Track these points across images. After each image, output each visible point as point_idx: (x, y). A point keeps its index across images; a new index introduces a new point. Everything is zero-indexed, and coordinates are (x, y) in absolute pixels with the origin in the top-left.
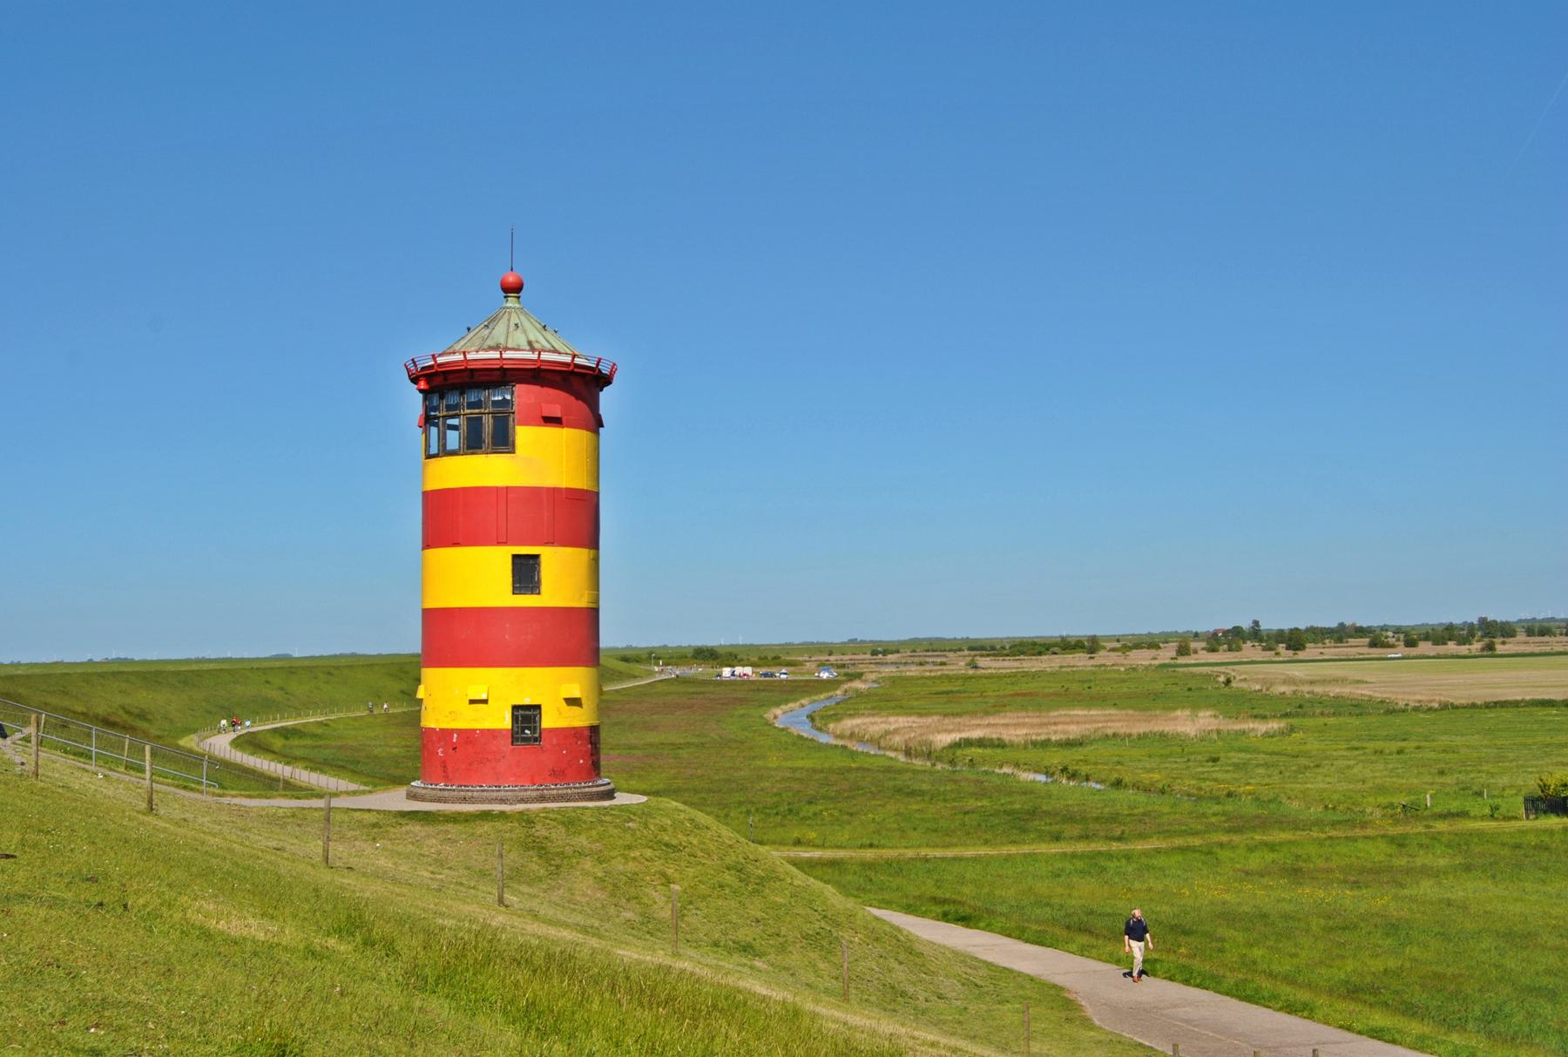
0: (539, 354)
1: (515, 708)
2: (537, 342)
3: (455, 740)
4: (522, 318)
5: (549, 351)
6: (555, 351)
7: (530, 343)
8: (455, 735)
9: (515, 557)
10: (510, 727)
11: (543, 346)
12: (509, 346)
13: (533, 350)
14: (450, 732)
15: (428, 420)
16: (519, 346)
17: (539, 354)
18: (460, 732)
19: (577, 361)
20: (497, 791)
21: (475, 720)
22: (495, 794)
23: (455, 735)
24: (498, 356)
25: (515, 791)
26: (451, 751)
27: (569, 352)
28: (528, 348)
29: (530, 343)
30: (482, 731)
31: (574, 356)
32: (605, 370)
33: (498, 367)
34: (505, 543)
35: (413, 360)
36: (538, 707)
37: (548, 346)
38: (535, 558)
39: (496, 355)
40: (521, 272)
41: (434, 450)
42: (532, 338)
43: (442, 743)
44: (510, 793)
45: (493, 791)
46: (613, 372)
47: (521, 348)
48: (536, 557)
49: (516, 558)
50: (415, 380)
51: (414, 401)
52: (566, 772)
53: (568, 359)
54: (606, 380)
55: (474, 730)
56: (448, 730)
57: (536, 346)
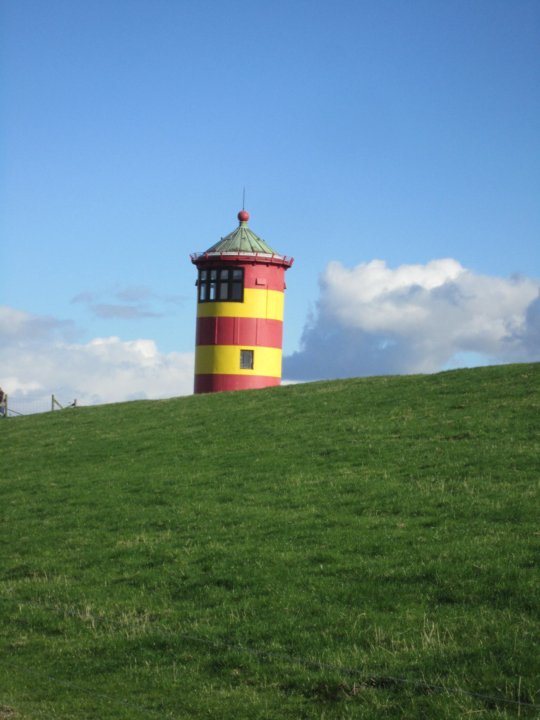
0: (257, 254)
2: (256, 247)
4: (248, 234)
5: (261, 252)
6: (265, 252)
7: (252, 248)
9: (242, 351)
11: (258, 249)
12: (242, 249)
13: (253, 251)
15: (199, 283)
16: (247, 249)
17: (257, 254)
19: (275, 257)
24: (237, 255)
27: (271, 252)
28: (251, 250)
29: (252, 248)
31: (273, 254)
32: (288, 260)
33: (235, 260)
34: (236, 344)
35: (195, 253)
37: (261, 249)
38: (252, 352)
39: (236, 254)
40: (249, 212)
41: (202, 298)
42: (253, 245)
46: (292, 260)
47: (248, 250)
48: (252, 352)
50: (194, 262)
51: (193, 272)
53: (270, 256)
54: (289, 267)
57: (255, 249)
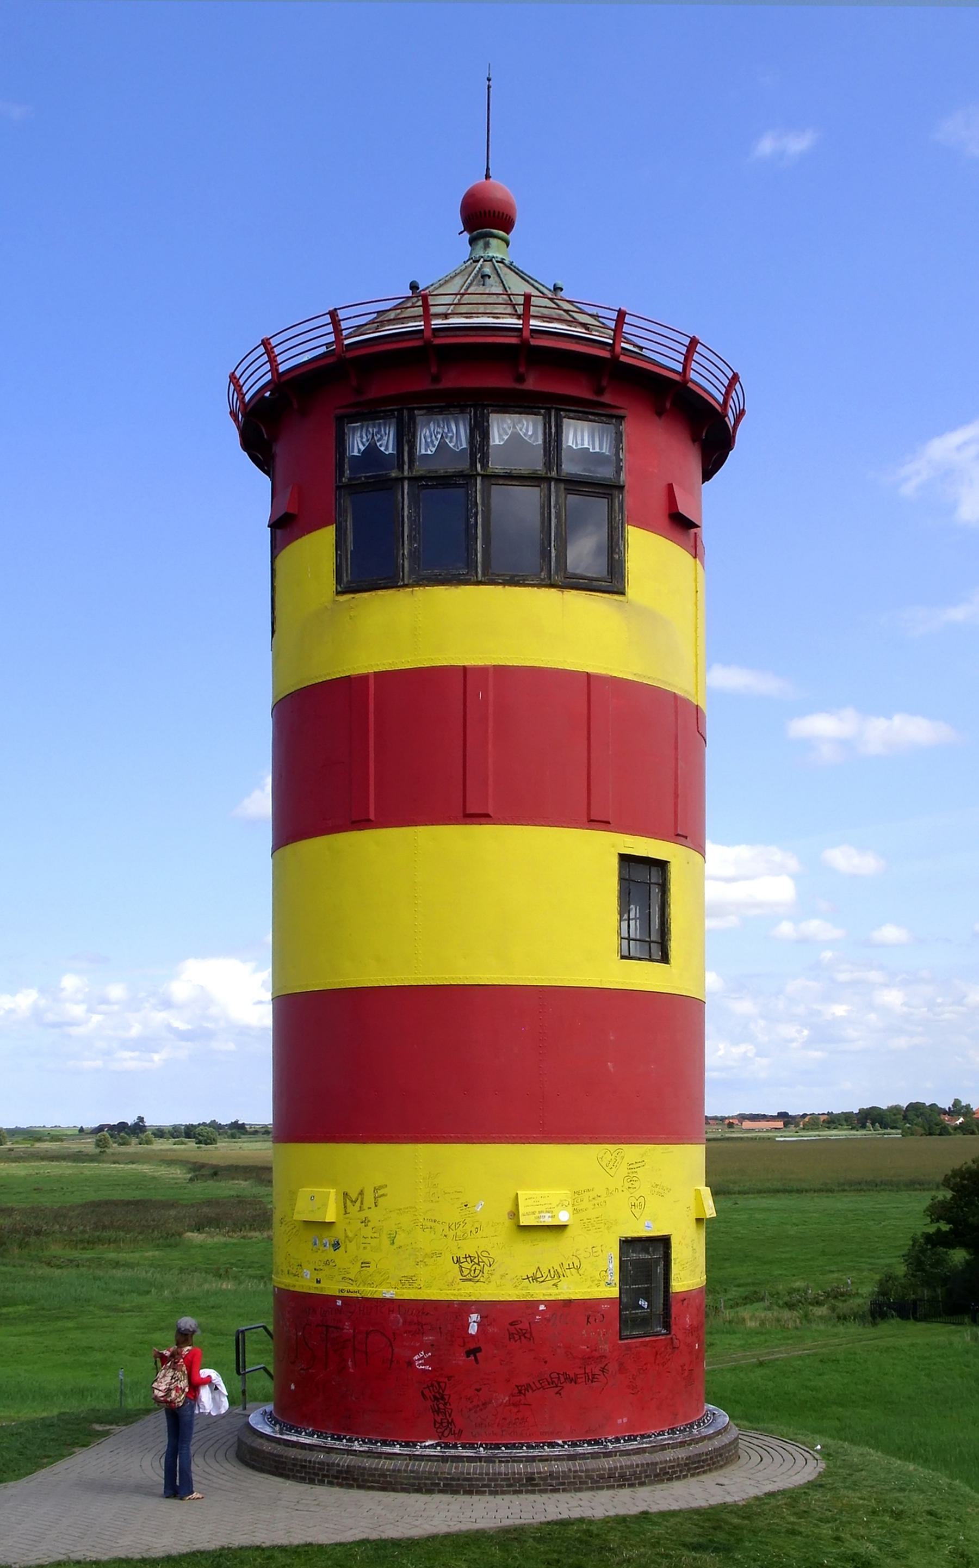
1: (627, 1244)
3: (473, 1329)
8: (474, 1317)
10: (614, 1292)
14: (465, 1307)
18: (490, 1310)
20: (594, 1456)
21: (535, 1279)
22: (591, 1464)
23: (474, 1317)
25: (643, 1451)
26: (460, 1358)
30: (551, 1304)
36: (665, 1241)
43: (428, 1338)
44: (636, 1459)
45: (583, 1456)
49: (626, 860)
52: (558, 1395)
55: (530, 1306)
56: (450, 1303)
